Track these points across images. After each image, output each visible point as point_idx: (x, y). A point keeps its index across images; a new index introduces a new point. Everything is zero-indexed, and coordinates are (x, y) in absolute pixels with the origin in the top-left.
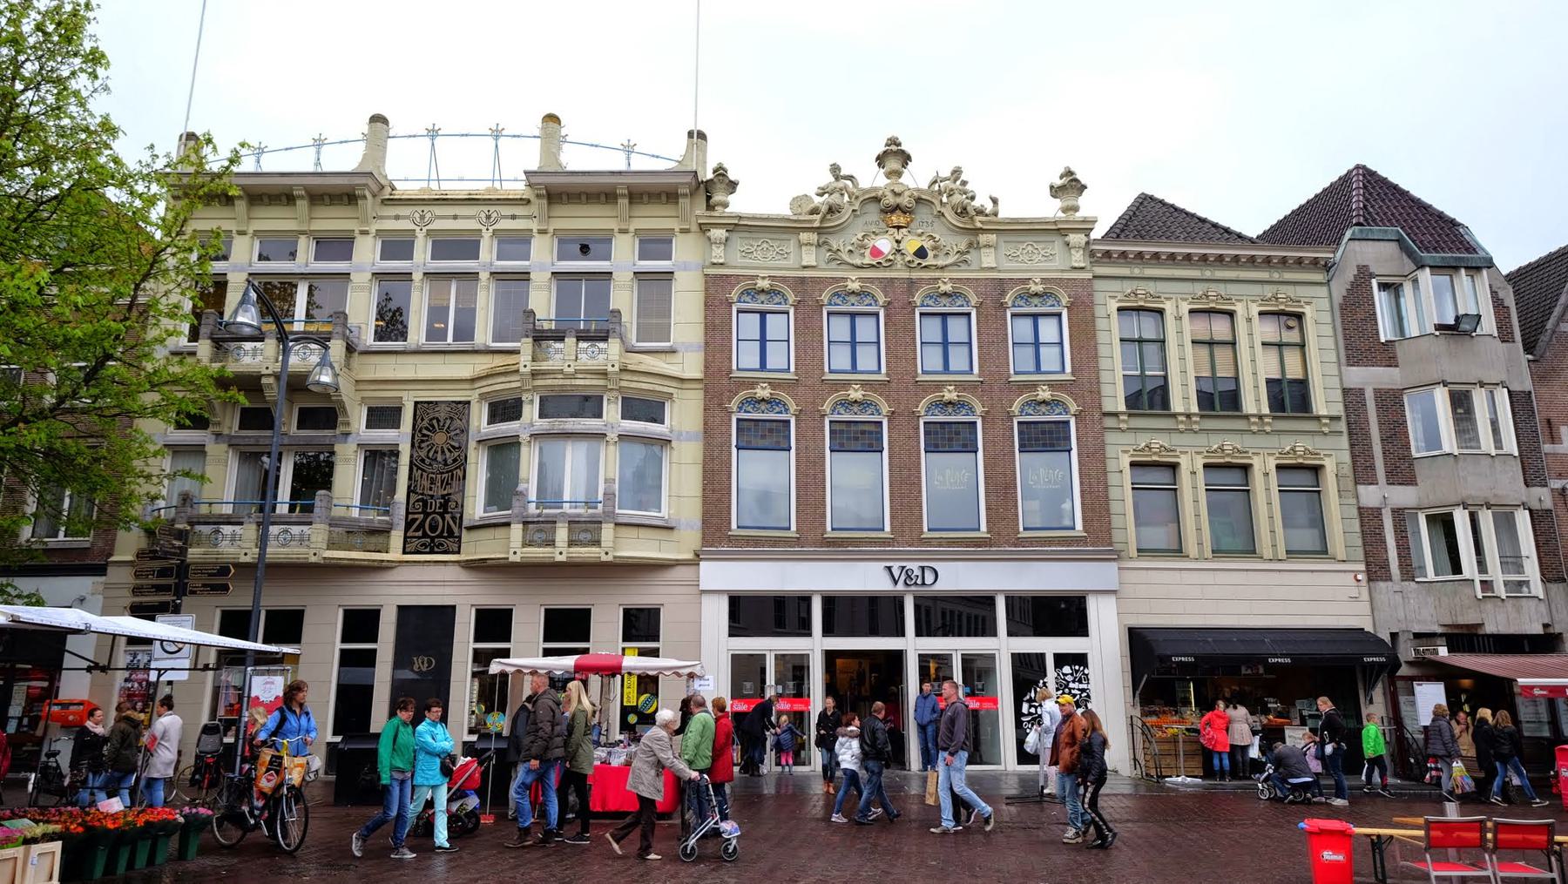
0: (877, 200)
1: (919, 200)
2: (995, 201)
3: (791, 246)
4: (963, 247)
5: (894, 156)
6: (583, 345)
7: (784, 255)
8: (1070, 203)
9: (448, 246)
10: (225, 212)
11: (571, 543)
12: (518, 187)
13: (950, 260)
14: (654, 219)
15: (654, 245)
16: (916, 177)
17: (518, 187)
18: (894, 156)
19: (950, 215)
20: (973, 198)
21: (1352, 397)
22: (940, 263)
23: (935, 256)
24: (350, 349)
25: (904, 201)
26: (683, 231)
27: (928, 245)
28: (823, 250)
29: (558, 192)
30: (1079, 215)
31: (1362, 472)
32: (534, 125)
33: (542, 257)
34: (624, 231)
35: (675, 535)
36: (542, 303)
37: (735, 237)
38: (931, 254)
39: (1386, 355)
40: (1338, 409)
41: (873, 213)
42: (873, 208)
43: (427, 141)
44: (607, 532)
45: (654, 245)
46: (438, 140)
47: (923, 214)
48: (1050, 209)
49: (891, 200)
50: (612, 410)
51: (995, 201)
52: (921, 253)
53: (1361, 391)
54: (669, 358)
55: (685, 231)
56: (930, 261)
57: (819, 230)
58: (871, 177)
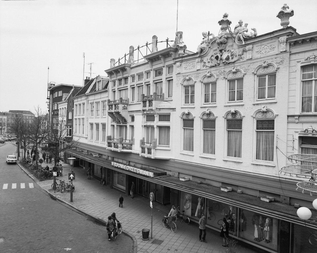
1: (227, 38)
4: (240, 53)
5: (225, 23)
8: (285, 21)
17: (143, 61)
18: (225, 23)
19: (236, 40)
23: (232, 58)
28: (202, 63)
34: (164, 67)
38: (230, 58)
41: (216, 47)
47: (230, 43)
49: (218, 41)
50: (157, 118)
51: (254, 30)
52: (228, 59)
56: (231, 60)
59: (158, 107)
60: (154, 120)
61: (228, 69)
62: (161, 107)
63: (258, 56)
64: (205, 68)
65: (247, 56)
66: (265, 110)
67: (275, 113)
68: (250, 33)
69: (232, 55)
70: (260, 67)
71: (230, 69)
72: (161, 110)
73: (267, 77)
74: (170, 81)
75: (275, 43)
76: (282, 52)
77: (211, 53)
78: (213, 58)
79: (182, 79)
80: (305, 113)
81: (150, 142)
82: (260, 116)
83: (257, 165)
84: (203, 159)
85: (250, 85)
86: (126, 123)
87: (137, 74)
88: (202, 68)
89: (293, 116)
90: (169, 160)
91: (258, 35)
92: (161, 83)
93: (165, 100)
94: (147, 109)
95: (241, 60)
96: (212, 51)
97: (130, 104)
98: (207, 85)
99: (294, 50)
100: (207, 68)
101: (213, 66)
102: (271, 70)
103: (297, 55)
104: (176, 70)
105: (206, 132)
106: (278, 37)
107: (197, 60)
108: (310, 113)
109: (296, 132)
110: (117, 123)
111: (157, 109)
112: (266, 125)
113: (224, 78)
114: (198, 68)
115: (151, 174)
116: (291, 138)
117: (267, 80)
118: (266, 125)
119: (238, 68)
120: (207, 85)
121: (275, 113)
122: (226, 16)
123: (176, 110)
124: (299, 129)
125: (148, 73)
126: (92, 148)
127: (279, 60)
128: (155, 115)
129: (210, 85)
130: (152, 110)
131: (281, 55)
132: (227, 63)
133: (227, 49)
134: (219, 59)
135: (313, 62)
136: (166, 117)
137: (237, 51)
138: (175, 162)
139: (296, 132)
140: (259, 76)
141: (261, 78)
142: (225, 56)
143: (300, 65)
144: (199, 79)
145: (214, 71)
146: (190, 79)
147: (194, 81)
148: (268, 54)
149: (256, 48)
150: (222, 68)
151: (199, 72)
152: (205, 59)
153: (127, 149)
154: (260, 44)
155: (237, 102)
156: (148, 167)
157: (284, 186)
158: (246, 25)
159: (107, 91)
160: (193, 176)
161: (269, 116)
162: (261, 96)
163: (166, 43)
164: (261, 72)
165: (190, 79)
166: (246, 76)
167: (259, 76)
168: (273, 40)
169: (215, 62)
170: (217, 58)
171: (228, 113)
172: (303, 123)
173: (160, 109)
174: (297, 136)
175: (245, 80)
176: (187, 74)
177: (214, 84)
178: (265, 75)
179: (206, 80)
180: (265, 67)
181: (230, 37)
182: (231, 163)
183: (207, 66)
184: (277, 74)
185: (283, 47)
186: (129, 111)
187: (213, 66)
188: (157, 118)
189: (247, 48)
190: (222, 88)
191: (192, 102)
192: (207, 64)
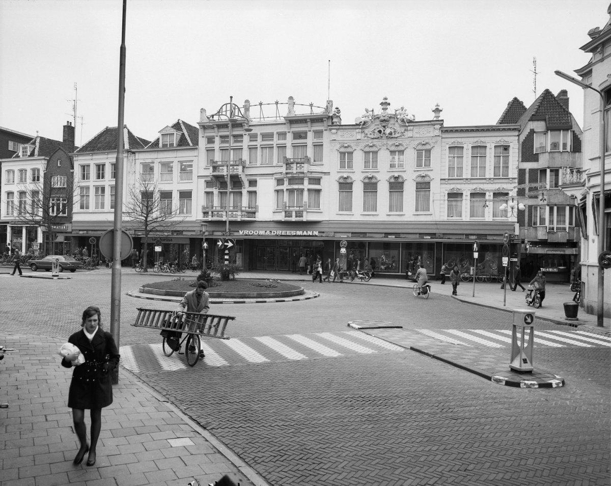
0: (378, 118)
1: (390, 118)
2: (414, 116)
3: (355, 133)
5: (385, 104)
6: (298, 165)
7: (352, 136)
9: (266, 136)
10: (212, 131)
11: (296, 217)
12: (283, 120)
13: (399, 135)
14: (318, 127)
15: (318, 134)
16: (391, 111)
17: (283, 120)
18: (385, 104)
19: (399, 121)
20: (407, 116)
21: (522, 172)
22: (396, 136)
24: (244, 167)
25: (386, 118)
26: (325, 130)
27: (392, 131)
28: (363, 133)
29: (292, 121)
30: (440, 119)
32: (286, 100)
33: (289, 140)
35: (322, 214)
36: (289, 154)
37: (339, 131)
38: (393, 134)
39: (535, 158)
40: (516, 176)
41: (378, 122)
42: (377, 120)
43: (259, 106)
44: (305, 213)
45: (318, 134)
46: (262, 106)
47: (392, 121)
48: (431, 116)
49: (382, 118)
50: (306, 182)
51: (414, 116)
52: (390, 134)
53: (525, 170)
54: (321, 166)
56: (393, 136)
57: (362, 128)
58: (379, 111)
59: (310, 171)
60: (283, 184)
61: (390, 142)
62: (313, 171)
63: (418, 135)
64: (366, 138)
65: (409, 134)
66: (424, 175)
67: (432, 178)
68: (410, 117)
69: (394, 132)
70: (420, 144)
71: (394, 142)
72: (313, 173)
73: (424, 151)
75: (431, 128)
76: (436, 136)
77: (373, 127)
78: (376, 131)
79: (338, 146)
80: (451, 178)
82: (419, 180)
83: (418, 215)
84: (365, 216)
85: (410, 156)
87: (261, 134)
88: (363, 138)
89: (444, 179)
90: (320, 222)
91: (416, 120)
92: (320, 146)
93: (311, 164)
95: (403, 137)
96: (373, 125)
97: (247, 166)
98: (367, 153)
99: (444, 136)
100: (369, 139)
101: (376, 138)
102: (428, 147)
103: (446, 139)
104: (327, 137)
105: (366, 194)
106: (434, 125)
107: (357, 130)
108: (454, 178)
109: (446, 190)
111: (308, 172)
112: (423, 186)
113: (387, 149)
114: (359, 137)
116: (443, 194)
117: (424, 154)
118: (423, 186)
119: (401, 142)
120: (367, 153)
121: (432, 178)
122: (437, 111)
123: (331, 174)
124: (449, 188)
125: (282, 135)
127: (434, 141)
128: (285, 179)
130: (303, 173)
131: (436, 138)
132: (390, 136)
133: (390, 126)
134: (382, 133)
135: (479, 145)
136: (317, 181)
137: (400, 130)
138: (329, 222)
139: (446, 190)
140: (341, 153)
141: (419, 153)
142: (388, 131)
143: (448, 146)
144: (360, 148)
145: (376, 142)
146: (348, 146)
147: (354, 148)
148: (426, 135)
149: (416, 129)
150: (385, 141)
152: (366, 131)
154: (418, 127)
158: (405, 110)
159: (196, 149)
160: (352, 233)
161: (427, 179)
162: (419, 165)
163: (310, 107)
164: (420, 147)
165: (348, 146)
166: (407, 150)
167: (341, 153)
168: (429, 126)
170: (380, 132)
171: (391, 178)
172: (450, 184)
173: (311, 172)
174: (447, 192)
175: (354, 154)
176: (346, 142)
177: (375, 153)
178: (369, 152)
179: (367, 149)
180: (371, 146)
181: (394, 117)
183: (368, 137)
184: (405, 152)
185: (438, 132)
186: (246, 175)
187: (376, 138)
188: (306, 182)
189: (409, 128)
192: (369, 135)
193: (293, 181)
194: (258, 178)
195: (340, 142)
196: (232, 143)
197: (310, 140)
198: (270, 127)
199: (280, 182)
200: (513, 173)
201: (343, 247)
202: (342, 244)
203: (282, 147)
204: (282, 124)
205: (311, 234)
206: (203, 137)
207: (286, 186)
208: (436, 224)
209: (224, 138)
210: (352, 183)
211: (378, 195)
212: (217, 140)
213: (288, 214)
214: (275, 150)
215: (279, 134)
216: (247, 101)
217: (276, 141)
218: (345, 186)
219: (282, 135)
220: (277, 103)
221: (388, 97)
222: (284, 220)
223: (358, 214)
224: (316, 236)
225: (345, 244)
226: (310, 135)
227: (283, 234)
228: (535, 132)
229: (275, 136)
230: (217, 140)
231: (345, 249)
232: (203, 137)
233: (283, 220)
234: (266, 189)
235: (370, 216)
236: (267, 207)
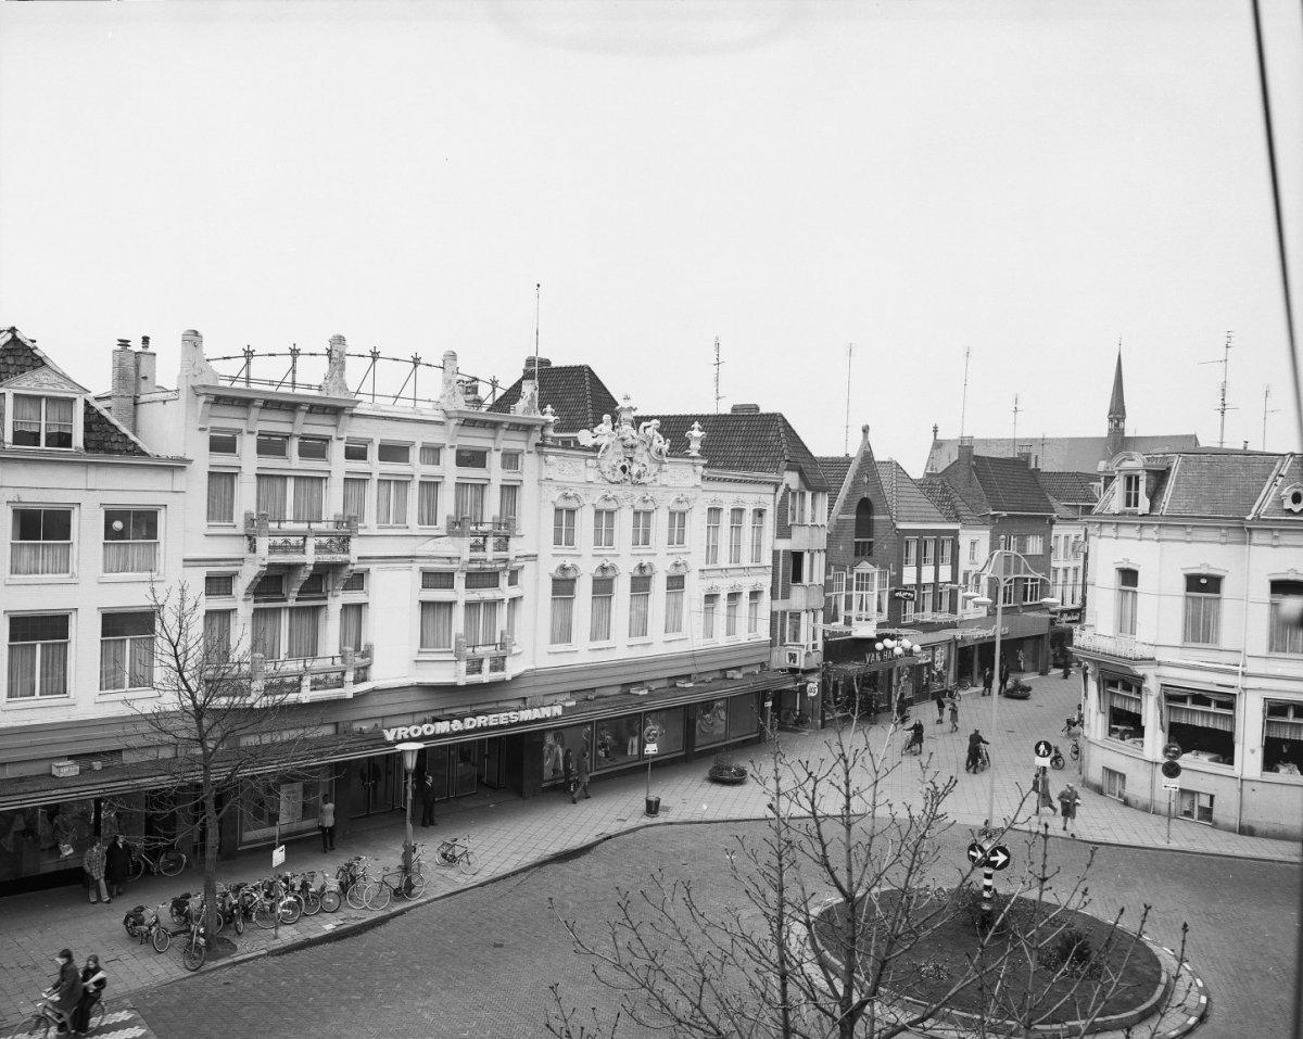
7: (578, 472)
15: (510, 460)
31: (774, 596)
45: (510, 460)
46: (379, 361)
52: (639, 476)
55: (529, 452)
56: (642, 480)
74: (510, 491)
79: (556, 495)
81: (498, 640)
86: (326, 598)
94: (490, 558)
110: (255, 601)
114: (590, 478)
115: (558, 710)
126: (59, 737)
129: (605, 516)
132: (638, 483)
145: (615, 491)
150: (628, 489)
151: (590, 486)
153: (327, 688)
155: (642, 550)
156: (441, 713)
157: (698, 661)
160: (572, 692)
169: (619, 476)
170: (624, 469)
182: (639, 647)
190: (624, 523)
191: (570, 542)
193: (473, 582)
194: (373, 568)
195: (559, 484)
196: (294, 462)
197: (495, 472)
198: (407, 426)
199: (432, 579)
200: (767, 560)
201: (652, 741)
202: (649, 735)
203: (430, 487)
204: (437, 423)
205: (549, 715)
206: (201, 429)
207: (460, 593)
208: (693, 656)
209: (271, 445)
210: (574, 580)
211: (613, 607)
212: (247, 445)
213: (475, 665)
214: (414, 492)
215: (426, 449)
216: (341, 340)
217: (416, 467)
218: (563, 586)
219: (432, 453)
220: (416, 362)
221: (630, 394)
222: (464, 683)
223: (582, 652)
224: (557, 717)
225: (655, 735)
226: (494, 460)
227: (491, 724)
228: (790, 490)
229: (415, 454)
230: (247, 445)
231: (655, 745)
232: (201, 429)
233: (462, 683)
234: (392, 602)
235: (604, 652)
236: (393, 646)
